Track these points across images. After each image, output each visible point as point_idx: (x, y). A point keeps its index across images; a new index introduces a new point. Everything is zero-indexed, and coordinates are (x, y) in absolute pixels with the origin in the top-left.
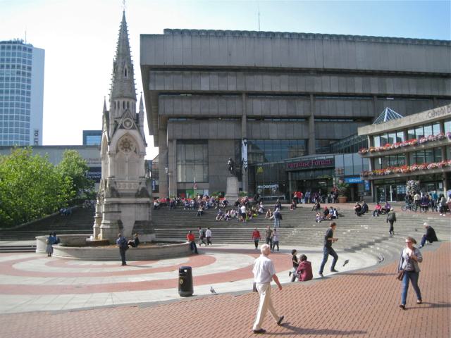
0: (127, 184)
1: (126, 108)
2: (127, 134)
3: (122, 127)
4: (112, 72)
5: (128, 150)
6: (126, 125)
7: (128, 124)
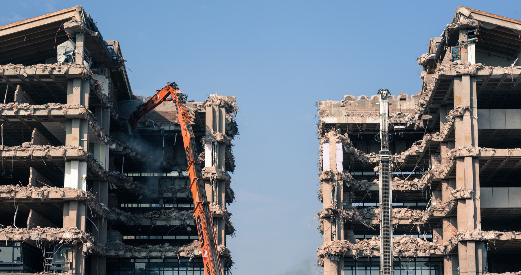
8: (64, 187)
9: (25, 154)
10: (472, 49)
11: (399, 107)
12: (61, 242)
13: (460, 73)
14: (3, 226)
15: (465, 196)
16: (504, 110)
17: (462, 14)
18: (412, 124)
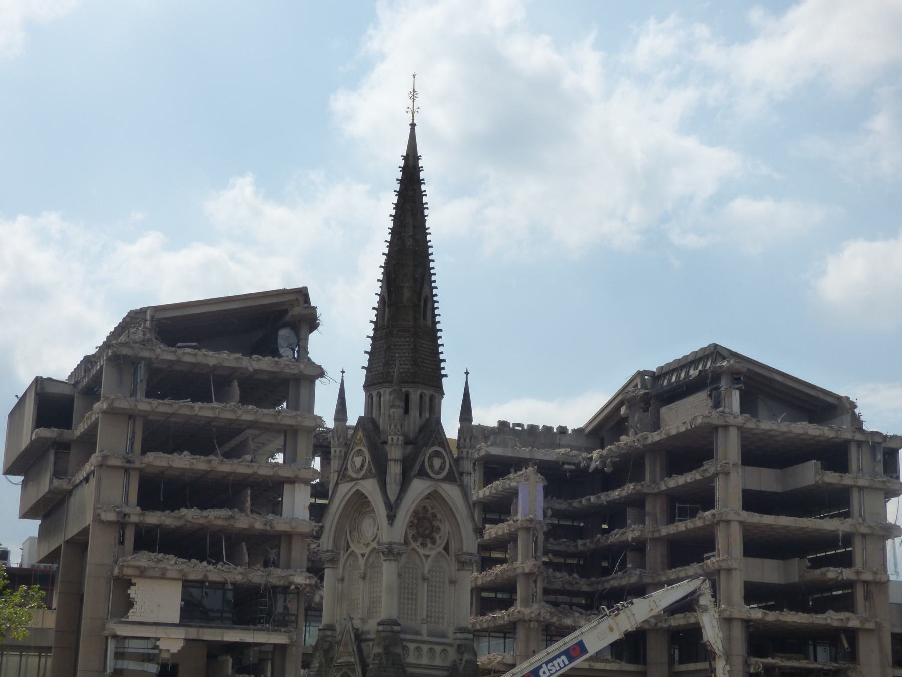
0: (425, 648)
1: (428, 415)
2: (429, 497)
3: (423, 474)
4: (375, 301)
5: (429, 541)
6: (432, 467)
7: (437, 463)
8: (281, 515)
9: (249, 471)
10: (736, 396)
13: (728, 422)
14: (214, 561)
17: (719, 353)
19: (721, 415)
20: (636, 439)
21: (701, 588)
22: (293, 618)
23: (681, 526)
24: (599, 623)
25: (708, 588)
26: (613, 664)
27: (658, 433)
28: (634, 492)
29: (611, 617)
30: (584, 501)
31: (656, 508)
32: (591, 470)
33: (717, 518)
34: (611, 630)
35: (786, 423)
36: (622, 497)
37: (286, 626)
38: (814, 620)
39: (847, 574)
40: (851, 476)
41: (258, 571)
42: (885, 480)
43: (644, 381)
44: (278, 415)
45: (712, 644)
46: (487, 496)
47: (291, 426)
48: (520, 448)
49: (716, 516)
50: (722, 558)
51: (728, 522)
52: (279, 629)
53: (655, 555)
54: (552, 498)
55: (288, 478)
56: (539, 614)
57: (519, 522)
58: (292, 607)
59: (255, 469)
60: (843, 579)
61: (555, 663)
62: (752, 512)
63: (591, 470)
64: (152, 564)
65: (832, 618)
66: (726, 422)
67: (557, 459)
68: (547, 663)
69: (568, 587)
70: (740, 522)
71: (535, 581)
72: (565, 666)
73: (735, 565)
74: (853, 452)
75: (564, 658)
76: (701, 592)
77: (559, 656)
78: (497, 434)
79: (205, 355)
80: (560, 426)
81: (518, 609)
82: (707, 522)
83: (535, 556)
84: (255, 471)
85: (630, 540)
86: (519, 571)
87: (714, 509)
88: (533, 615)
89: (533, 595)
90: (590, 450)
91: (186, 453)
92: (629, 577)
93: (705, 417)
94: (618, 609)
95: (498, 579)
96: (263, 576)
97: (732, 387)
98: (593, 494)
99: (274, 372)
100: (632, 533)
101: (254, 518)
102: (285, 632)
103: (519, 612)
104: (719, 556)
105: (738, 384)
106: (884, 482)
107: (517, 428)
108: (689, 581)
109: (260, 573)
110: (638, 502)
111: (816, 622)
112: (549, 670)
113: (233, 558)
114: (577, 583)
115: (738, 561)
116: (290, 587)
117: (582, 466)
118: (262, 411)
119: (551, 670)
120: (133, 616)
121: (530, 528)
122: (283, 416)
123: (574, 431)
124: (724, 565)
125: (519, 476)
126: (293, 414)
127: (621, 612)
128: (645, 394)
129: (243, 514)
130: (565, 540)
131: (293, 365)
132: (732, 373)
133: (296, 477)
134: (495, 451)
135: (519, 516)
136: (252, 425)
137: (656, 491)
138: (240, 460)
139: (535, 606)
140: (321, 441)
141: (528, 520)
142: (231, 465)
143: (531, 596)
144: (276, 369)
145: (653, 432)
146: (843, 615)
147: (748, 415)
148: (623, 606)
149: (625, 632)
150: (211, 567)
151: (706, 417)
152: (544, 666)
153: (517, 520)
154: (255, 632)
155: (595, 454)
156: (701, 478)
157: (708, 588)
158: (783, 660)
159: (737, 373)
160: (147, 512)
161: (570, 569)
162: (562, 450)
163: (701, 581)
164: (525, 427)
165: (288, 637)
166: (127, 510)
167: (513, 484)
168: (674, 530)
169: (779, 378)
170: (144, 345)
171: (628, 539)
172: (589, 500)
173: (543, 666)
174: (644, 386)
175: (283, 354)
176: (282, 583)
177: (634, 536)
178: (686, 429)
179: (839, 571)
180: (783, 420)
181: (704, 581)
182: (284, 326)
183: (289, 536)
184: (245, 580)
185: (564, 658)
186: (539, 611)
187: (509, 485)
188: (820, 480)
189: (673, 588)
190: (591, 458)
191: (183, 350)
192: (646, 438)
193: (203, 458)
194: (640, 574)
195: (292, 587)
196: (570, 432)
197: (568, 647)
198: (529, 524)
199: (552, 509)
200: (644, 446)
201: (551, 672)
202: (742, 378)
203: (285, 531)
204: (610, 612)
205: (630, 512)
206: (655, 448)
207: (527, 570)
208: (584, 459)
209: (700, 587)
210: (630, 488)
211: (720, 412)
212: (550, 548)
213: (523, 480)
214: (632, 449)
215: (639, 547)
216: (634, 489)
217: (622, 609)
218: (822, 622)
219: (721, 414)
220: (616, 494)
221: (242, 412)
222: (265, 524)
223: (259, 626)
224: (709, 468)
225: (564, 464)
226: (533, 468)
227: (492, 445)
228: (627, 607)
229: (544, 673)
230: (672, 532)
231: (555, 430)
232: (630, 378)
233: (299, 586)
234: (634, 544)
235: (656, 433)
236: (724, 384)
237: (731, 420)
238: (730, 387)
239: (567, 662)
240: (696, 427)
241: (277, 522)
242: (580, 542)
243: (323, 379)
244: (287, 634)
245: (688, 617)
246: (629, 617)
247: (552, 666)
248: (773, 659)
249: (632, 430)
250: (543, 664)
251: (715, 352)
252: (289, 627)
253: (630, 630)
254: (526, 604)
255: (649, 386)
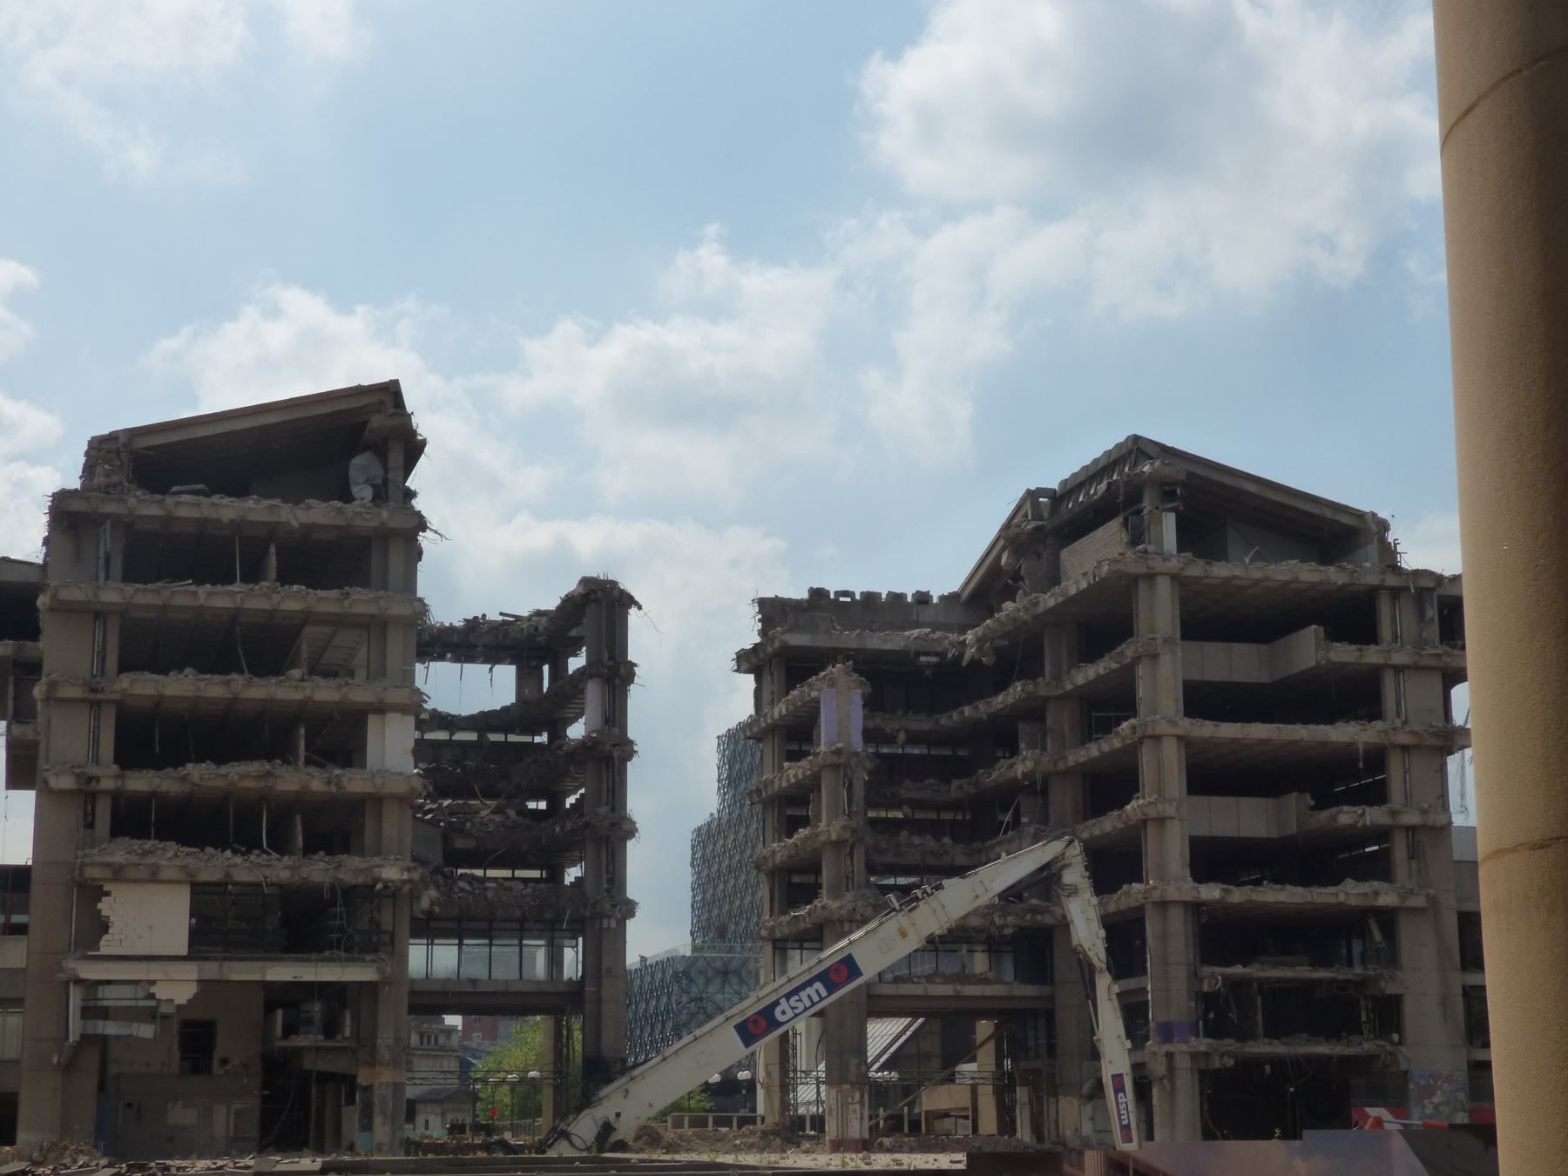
9: (298, 696)
10: (1169, 522)
11: (914, 617)
12: (379, 886)
13: (1153, 568)
14: (244, 849)
15: (1167, 814)
16: (1200, 642)
18: (957, 654)
19: (1141, 557)
20: (1021, 606)
21: (1067, 854)
22: (386, 938)
23: (1094, 750)
24: (880, 924)
25: (1078, 855)
26: (996, 986)
27: (1052, 595)
28: (1024, 695)
29: (903, 913)
30: (955, 716)
31: (1061, 720)
32: (964, 664)
33: (1139, 734)
34: (903, 934)
35: (1260, 564)
36: (1006, 706)
37: (375, 950)
38: (1315, 897)
39: (1374, 816)
40: (1377, 648)
41: (320, 862)
42: (1440, 652)
43: (1036, 506)
44: (346, 598)
45: (1087, 950)
46: (785, 716)
47: (373, 616)
48: (841, 633)
49: (1137, 729)
50: (1149, 799)
51: (1157, 738)
52: (361, 956)
53: (1064, 798)
54: (906, 712)
55: (371, 704)
56: (854, 909)
57: (820, 757)
58: (386, 919)
59: (308, 692)
60: (1364, 824)
61: (803, 995)
62: (1201, 720)
63: (964, 664)
64: (134, 859)
65: (1350, 893)
66: (1148, 568)
67: (905, 646)
68: (788, 996)
69: (931, 860)
70: (1179, 738)
71: (851, 854)
72: (822, 999)
73: (1170, 810)
74: (1384, 607)
75: (818, 985)
76: (1066, 861)
77: (809, 983)
78: (806, 610)
79: (213, 504)
80: (917, 592)
81: (826, 902)
82: (1128, 742)
83: (850, 812)
84: (308, 695)
85: (1019, 775)
86: (823, 838)
87: (1135, 717)
88: (843, 912)
89: (847, 878)
90: (963, 630)
91: (188, 670)
92: (1020, 839)
93: (1112, 562)
94: (917, 899)
95: (800, 852)
96: (328, 870)
97: (1160, 507)
98: (968, 703)
99: (338, 527)
100: (1022, 765)
101: (308, 774)
102: (373, 961)
103: (823, 908)
104: (1144, 798)
105: (1173, 502)
106: (1438, 656)
107: (841, 599)
108: (1043, 845)
109: (322, 865)
110: (1034, 712)
111: (1320, 901)
112: (793, 1008)
113: (280, 844)
114: (946, 852)
115: (1175, 803)
116: (375, 886)
117: (950, 655)
118: (316, 594)
119: (796, 1008)
120: (107, 946)
121: (839, 765)
122: (354, 600)
123: (942, 598)
124: (1152, 813)
125: (820, 680)
126: (372, 596)
127: (921, 903)
128: (1036, 529)
129: (291, 768)
130: (932, 781)
131: (368, 513)
132: (1163, 484)
133: (381, 701)
134: (799, 640)
135: (823, 748)
136: (307, 617)
137: (1059, 692)
138: (282, 678)
139: (849, 896)
140: (501, 637)
141: (832, 752)
142: (267, 686)
143: (844, 880)
144: (341, 522)
145: (1045, 593)
146: (1366, 887)
147: (1189, 555)
148: (925, 892)
149: (929, 936)
150: (238, 860)
151: (1115, 561)
152: (783, 1001)
153: (819, 753)
154: (319, 964)
155: (970, 636)
156: (1118, 665)
157: (1078, 855)
158: (1265, 968)
159: (1168, 484)
160: (128, 773)
161: (935, 828)
162: (916, 632)
163: (1066, 843)
164: (858, 597)
165: (378, 969)
166: (93, 770)
167: (814, 694)
168: (1084, 756)
169: (1251, 488)
170: (108, 493)
171: (1017, 777)
172: (962, 713)
173: (781, 1001)
174: (1037, 514)
175: (356, 496)
176: (360, 880)
177: (1025, 771)
178: (1089, 584)
179: (1360, 812)
180: (1252, 561)
181: (1070, 842)
182: (365, 449)
183: (378, 800)
184: (297, 878)
185: (818, 985)
186: (853, 904)
187: (809, 695)
188: (1323, 658)
189: (1016, 857)
190: (964, 641)
191: (176, 498)
192: (1036, 604)
193: (218, 678)
194: (1036, 834)
195: (379, 886)
196: (935, 600)
197: (827, 966)
198: (835, 759)
199: (907, 731)
200: (1035, 617)
201: (797, 1011)
202: (1178, 491)
203: (369, 794)
204: (901, 905)
205: (1024, 729)
206: (1056, 618)
207: (834, 837)
208: (951, 643)
209: (1063, 854)
210: (1015, 692)
211: (1141, 552)
212: (903, 797)
213: (825, 687)
214: (1018, 623)
215: (1037, 787)
216: (1023, 690)
217: (923, 898)
218: (1332, 900)
219: (1141, 555)
220: (1001, 700)
221: (282, 597)
222: (329, 783)
223: (327, 954)
224: (1128, 650)
225: (918, 654)
226: (844, 664)
227: (790, 630)
228: (932, 894)
229: (783, 1013)
230: (1082, 760)
231: (909, 599)
232: (1017, 502)
233: (390, 884)
234: (1026, 783)
235: (1049, 594)
236: (1147, 504)
237: (1157, 565)
238: (1157, 508)
239: (824, 993)
240: (1102, 580)
241: (350, 779)
242: (955, 783)
243: (428, 533)
244: (375, 965)
245: (1107, 903)
246: (935, 911)
247: (797, 1001)
248: (1244, 967)
249: (1020, 591)
250: (781, 998)
251: (1137, 449)
252: (380, 953)
253: (938, 932)
254: (836, 893)
255: (1046, 515)
